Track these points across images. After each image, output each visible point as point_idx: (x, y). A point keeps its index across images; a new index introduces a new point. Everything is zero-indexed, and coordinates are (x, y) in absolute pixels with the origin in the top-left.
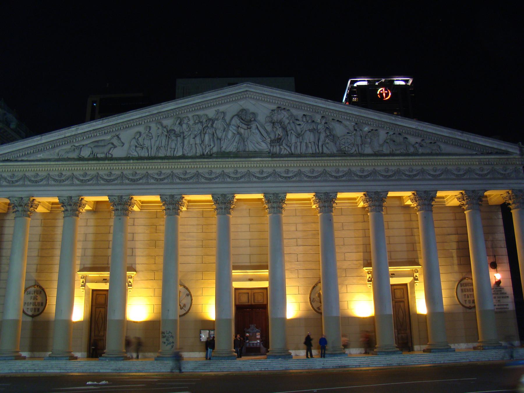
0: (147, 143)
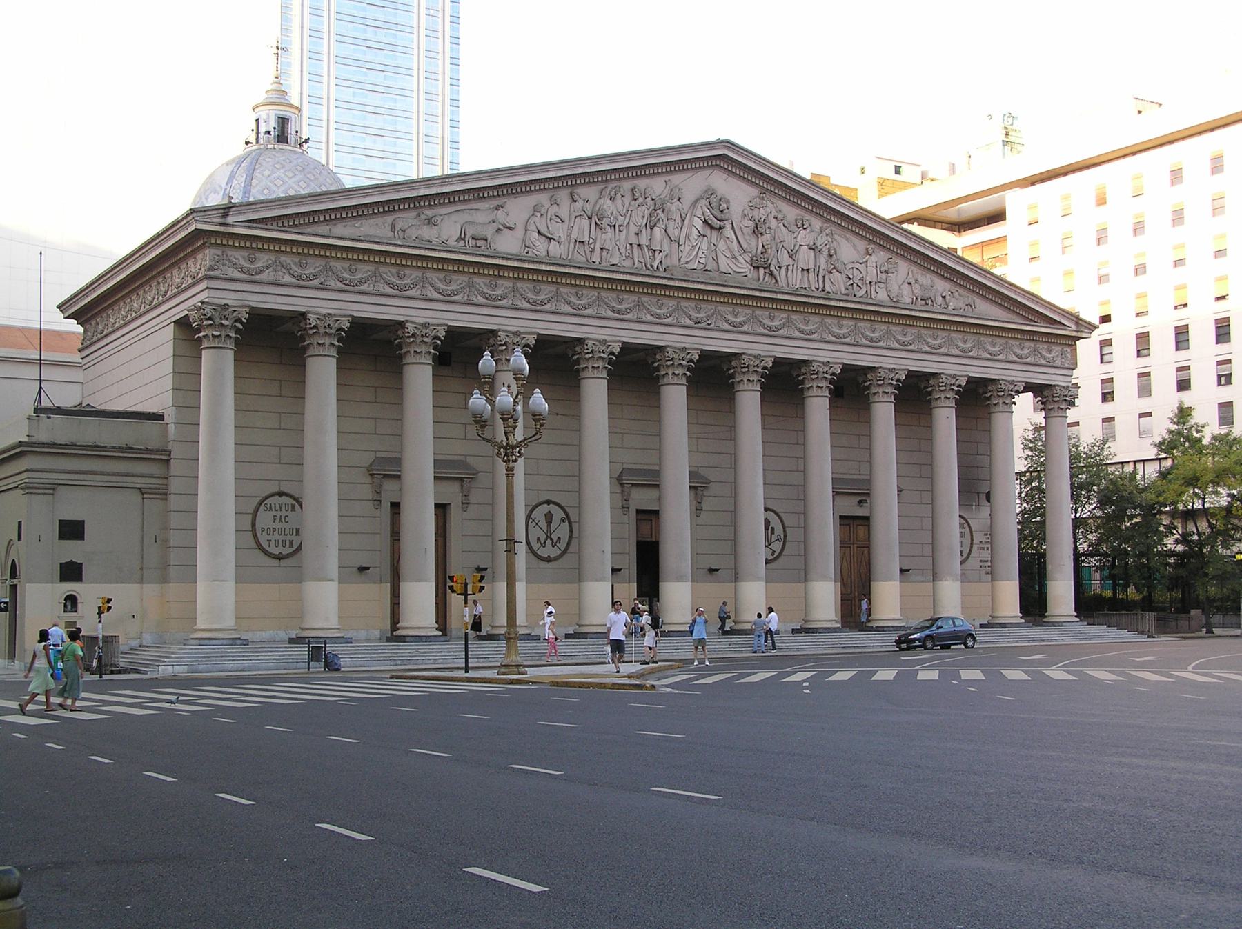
0: (559, 230)
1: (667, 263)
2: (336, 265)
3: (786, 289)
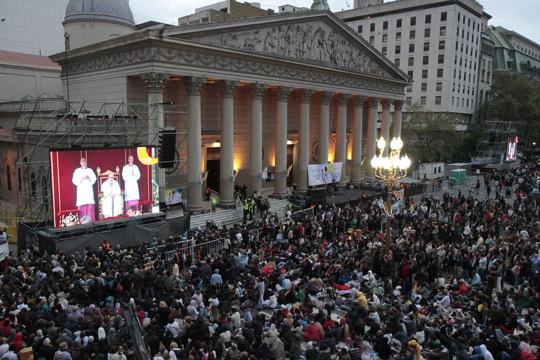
0: (275, 43)
1: (307, 57)
2: (201, 56)
3: (339, 68)
